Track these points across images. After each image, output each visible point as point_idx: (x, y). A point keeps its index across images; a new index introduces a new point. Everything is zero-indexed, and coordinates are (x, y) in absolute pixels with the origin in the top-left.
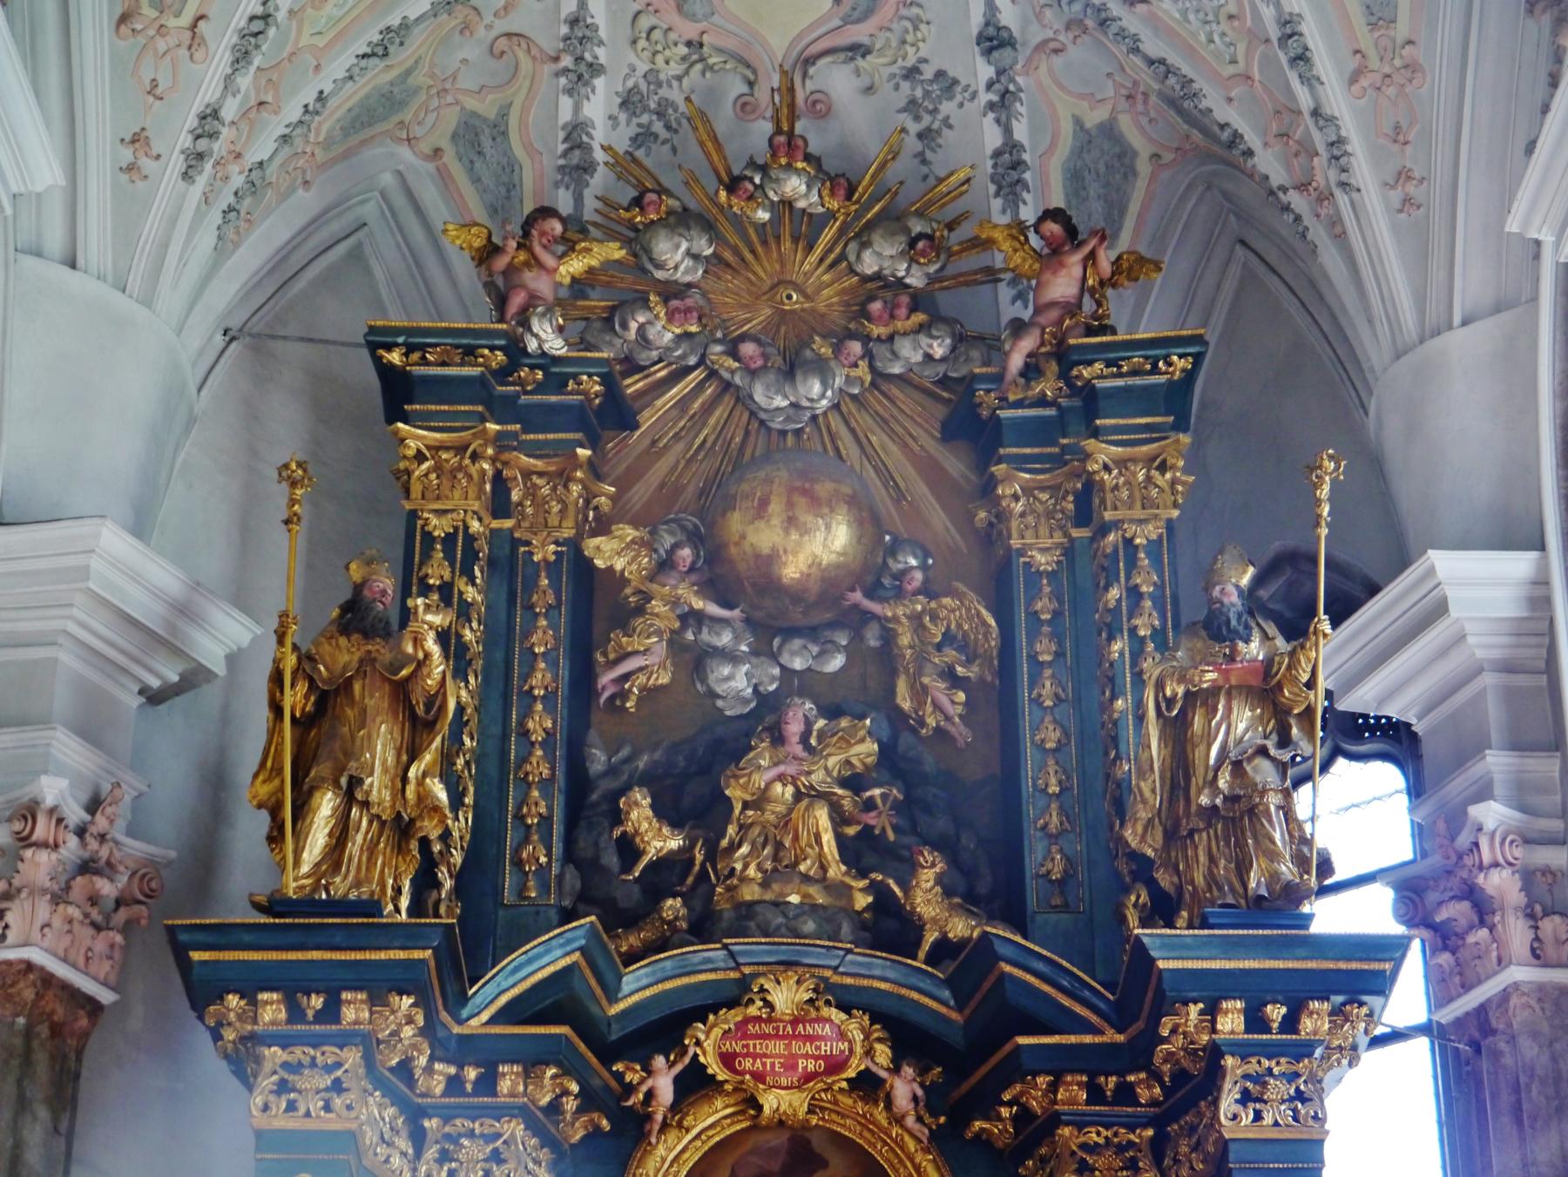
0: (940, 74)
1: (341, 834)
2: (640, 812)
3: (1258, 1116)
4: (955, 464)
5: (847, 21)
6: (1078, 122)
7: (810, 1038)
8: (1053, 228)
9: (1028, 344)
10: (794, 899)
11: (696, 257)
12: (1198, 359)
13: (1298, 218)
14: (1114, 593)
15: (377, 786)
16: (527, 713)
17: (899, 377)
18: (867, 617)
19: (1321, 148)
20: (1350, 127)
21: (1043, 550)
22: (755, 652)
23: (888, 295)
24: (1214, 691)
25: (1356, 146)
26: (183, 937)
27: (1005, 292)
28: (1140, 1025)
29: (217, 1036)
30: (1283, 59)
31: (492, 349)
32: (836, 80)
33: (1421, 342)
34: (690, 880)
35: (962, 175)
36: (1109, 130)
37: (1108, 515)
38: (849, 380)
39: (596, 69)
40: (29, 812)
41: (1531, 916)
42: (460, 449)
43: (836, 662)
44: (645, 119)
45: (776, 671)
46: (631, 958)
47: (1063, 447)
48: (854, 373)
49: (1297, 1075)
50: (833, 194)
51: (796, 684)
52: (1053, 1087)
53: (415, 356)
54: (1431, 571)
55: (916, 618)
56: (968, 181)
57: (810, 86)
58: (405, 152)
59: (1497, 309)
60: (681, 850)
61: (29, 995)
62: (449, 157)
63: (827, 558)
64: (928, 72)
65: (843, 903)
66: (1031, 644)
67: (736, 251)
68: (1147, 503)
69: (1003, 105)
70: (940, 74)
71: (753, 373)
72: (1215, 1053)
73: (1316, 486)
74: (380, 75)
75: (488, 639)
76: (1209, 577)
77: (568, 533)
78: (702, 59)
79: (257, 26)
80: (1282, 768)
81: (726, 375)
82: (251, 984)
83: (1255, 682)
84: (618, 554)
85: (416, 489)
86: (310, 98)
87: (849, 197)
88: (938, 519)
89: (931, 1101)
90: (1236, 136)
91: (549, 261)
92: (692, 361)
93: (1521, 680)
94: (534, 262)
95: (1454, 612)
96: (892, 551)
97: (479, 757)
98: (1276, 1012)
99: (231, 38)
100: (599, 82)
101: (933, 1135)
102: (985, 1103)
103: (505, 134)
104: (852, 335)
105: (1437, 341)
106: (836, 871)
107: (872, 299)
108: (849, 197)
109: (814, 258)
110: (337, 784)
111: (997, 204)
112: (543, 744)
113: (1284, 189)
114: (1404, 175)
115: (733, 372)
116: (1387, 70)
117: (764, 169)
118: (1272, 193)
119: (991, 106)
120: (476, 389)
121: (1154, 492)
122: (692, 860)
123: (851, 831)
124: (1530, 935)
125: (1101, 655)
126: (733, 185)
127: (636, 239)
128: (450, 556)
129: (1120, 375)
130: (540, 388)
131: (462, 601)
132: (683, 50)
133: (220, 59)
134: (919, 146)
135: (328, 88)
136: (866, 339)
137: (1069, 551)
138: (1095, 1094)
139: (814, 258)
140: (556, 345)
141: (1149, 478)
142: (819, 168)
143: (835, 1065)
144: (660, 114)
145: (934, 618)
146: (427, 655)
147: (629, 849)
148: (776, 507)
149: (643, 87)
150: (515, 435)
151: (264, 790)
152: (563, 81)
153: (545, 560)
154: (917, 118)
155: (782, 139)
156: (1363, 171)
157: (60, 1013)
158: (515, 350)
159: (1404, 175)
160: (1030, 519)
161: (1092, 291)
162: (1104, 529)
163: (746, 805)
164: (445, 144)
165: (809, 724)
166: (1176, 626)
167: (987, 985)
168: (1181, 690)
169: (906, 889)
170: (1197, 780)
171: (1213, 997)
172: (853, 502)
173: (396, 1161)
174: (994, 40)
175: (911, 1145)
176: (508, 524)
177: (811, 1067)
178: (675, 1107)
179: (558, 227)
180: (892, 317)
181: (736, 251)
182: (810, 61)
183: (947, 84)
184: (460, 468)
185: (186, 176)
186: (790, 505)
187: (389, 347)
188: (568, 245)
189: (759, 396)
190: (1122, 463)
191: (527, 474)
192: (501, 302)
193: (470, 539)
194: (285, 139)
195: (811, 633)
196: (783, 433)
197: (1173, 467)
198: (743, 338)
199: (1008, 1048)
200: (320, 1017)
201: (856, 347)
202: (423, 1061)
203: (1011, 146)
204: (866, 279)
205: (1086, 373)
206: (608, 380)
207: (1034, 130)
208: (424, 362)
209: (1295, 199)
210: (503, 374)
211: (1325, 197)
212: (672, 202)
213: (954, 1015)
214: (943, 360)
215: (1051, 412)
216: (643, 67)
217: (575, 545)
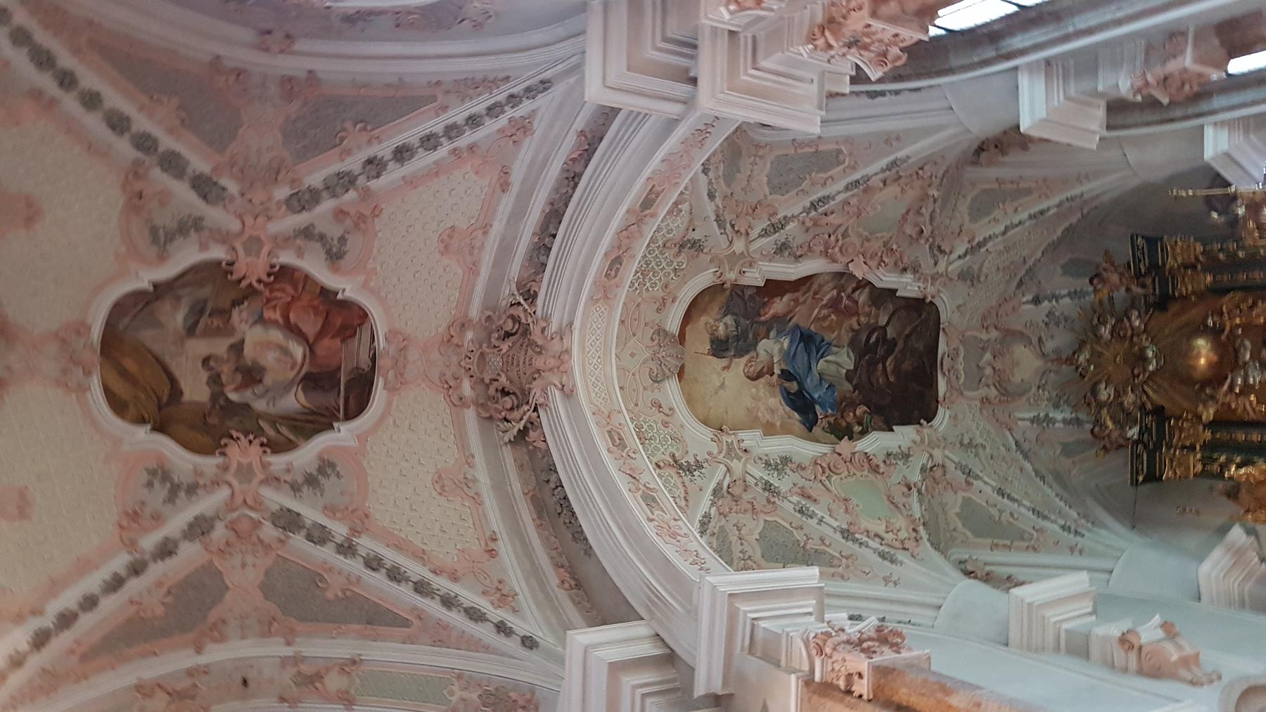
0: (1047, 316)
4: (1174, 307)
5: (1031, 343)
8: (1095, 281)
20: (1063, 197)
32: (1050, 346)
39: (1047, 415)
42: (1171, 461)
43: (1248, 343)
57: (1051, 354)
59: (1122, 148)
71: (1145, 370)
77: (1201, 428)
86: (1057, 500)
88: (1194, 314)
91: (1107, 431)
94: (1109, 435)
96: (1206, 326)
99: (1040, 520)
100: (1051, 415)
105: (1131, 164)
117: (1077, 368)
130: (1150, 434)
133: (1046, 524)
135: (1054, 494)
137: (1205, 270)
152: (1051, 426)
156: (1076, 191)
158: (1137, 442)
174: (1036, 301)
176: (1198, 447)
185: (1083, 536)
187: (1137, 481)
188: (1103, 426)
189: (1151, 368)
192: (1120, 446)
194: (1070, 507)
195: (1236, 352)
198: (1133, 372)
201: (1135, 339)
204: (1112, 335)
205: (1143, 270)
206: (1147, 414)
210: (1146, 447)
211: (1085, 202)
215: (1157, 279)
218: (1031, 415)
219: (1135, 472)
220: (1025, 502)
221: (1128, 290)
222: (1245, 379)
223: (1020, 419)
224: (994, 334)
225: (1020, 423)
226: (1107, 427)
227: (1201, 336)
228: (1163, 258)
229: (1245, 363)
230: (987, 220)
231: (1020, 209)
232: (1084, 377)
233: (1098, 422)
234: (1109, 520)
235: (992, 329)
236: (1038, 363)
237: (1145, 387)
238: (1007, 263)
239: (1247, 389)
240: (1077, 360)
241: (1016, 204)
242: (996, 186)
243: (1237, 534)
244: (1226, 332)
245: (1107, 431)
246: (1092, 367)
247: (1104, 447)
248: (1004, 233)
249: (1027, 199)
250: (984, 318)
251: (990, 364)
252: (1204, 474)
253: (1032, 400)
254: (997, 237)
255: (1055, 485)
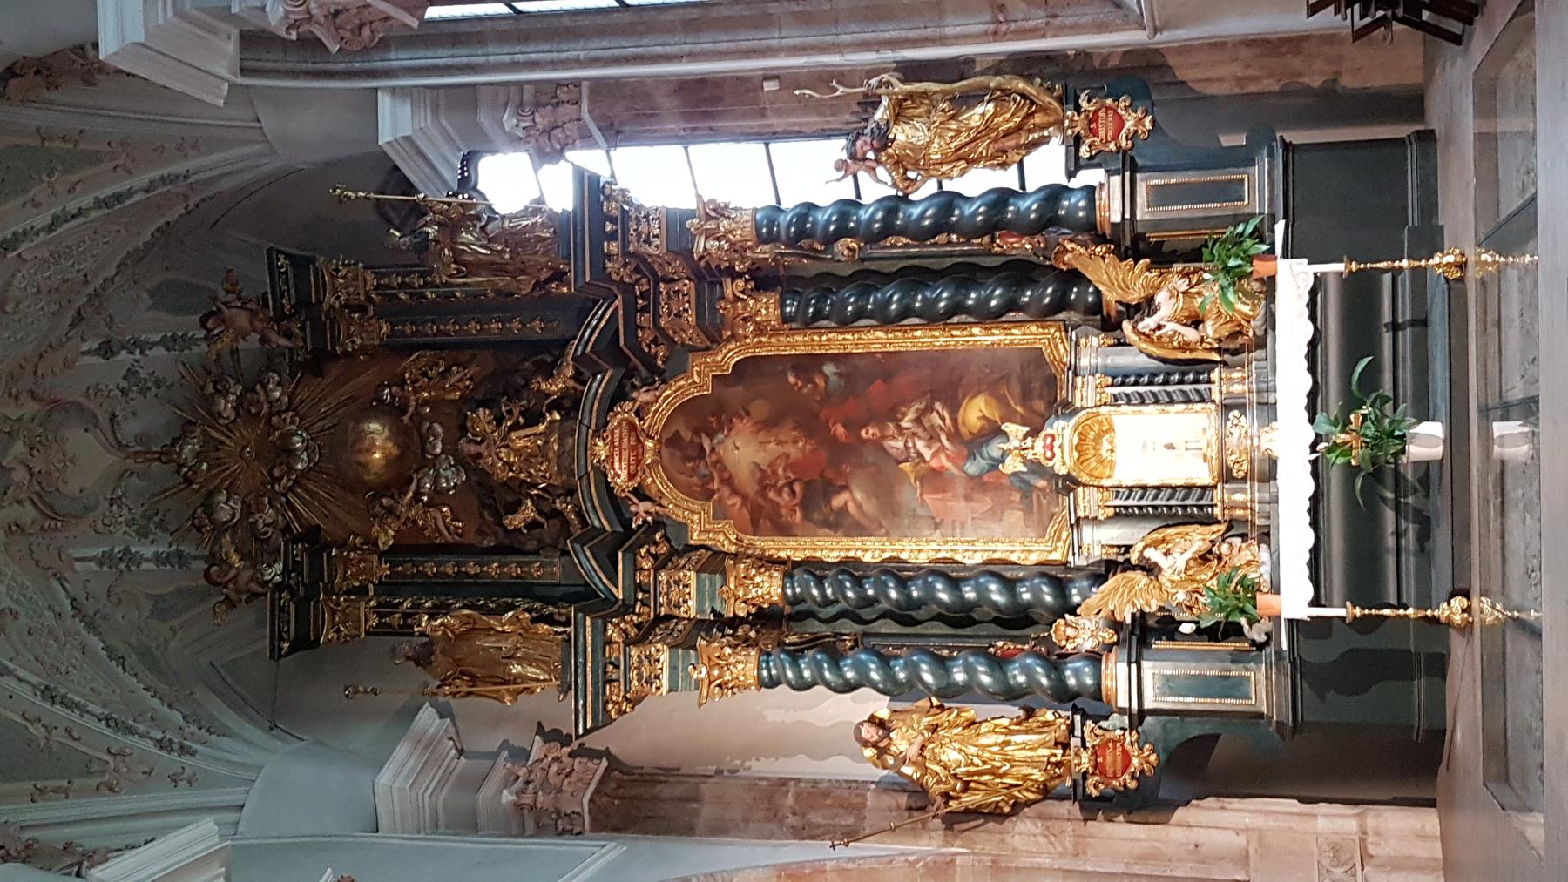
0: (125, 378)
1: (526, 660)
2: (516, 521)
3: (656, 236)
4: (334, 371)
5: (96, 425)
6: (150, 308)
7: (621, 439)
8: (210, 324)
9: (274, 337)
10: (556, 447)
11: (228, 500)
12: (279, 252)
13: (203, 200)
14: (402, 296)
15: (506, 645)
16: (466, 573)
17: (289, 398)
18: (416, 413)
19: (166, 189)
20: (156, 174)
21: (380, 328)
22: (434, 466)
23: (246, 404)
24: (452, 249)
25: (165, 171)
26: (581, 731)
27: (241, 345)
28: (614, 289)
29: (625, 712)
30: (119, 206)
31: (280, 598)
32: (130, 429)
33: (268, 142)
34: (546, 496)
35: (181, 367)
36: (152, 294)
37: (362, 298)
38: (292, 422)
39: (126, 551)
40: (519, 806)
41: (557, 104)
42: (333, 612)
43: (438, 429)
44: (152, 526)
45: (443, 457)
46: (583, 522)
47: (327, 318)
48: (288, 421)
49: (637, 218)
50: (191, 432)
51: (451, 448)
52: (642, 328)
53: (285, 635)
54: (389, 143)
55: (415, 391)
56: (184, 365)
58: (173, 644)
60: (532, 500)
61: (605, 799)
62: (176, 623)
63: (387, 433)
64: (124, 384)
65: (557, 425)
66: (427, 335)
67: (224, 480)
68: (355, 278)
69: (143, 346)
70: (125, 378)
71: (291, 469)
72: (626, 254)
73: (349, 198)
74: (132, 660)
75: (430, 596)
76: (396, 250)
77: (375, 557)
78: (120, 498)
79: (112, 723)
80: (490, 219)
81: (291, 483)
82: (601, 702)
83: (448, 231)
84: (386, 533)
85: (354, 632)
86: (148, 694)
87: (194, 424)
88: (366, 378)
89: (648, 383)
90: (158, 230)
91: (233, 572)
92: (283, 499)
93: (442, 103)
95: (408, 133)
96: (381, 401)
97: (489, 597)
98: (609, 227)
100: (133, 550)
101: (664, 382)
102: (649, 361)
103: (161, 596)
104: (269, 421)
106: (542, 427)
107: (249, 411)
108: (194, 424)
109: (228, 442)
110: (507, 664)
111: (195, 349)
112: (482, 567)
113: (186, 208)
114: (180, 148)
115: (289, 480)
116: (124, 155)
117: (180, 466)
118: (189, 213)
119: (142, 353)
120: (302, 606)
121: (350, 275)
122: (537, 495)
123: (521, 420)
124: (566, 105)
125: (433, 301)
126: (189, 481)
127: (220, 529)
128: (389, 615)
129: (288, 290)
130: (300, 574)
131: (411, 608)
132: (115, 507)
133: (132, 740)
134: (163, 388)
136: (270, 415)
137: (379, 316)
138: (644, 310)
139: (228, 442)
140: (278, 567)
141: (342, 278)
142: (179, 438)
143: (632, 427)
144: (150, 518)
145: (413, 382)
146: (442, 624)
147: (532, 525)
148: (361, 458)
149: (135, 527)
150: (325, 585)
151: (508, 698)
153: (389, 569)
154: (149, 389)
155: (163, 458)
156: (179, 168)
157: (613, 785)
158: (280, 587)
159: (180, 148)
160: (364, 335)
161: (244, 303)
162: (369, 299)
163: (511, 470)
164: (167, 625)
165: (470, 441)
166: (417, 266)
167: (594, 357)
168: (453, 266)
169: (548, 396)
170: (497, 259)
171: (600, 257)
172: (358, 421)
173: (680, 627)
174: (107, 350)
175: (667, 392)
177: (632, 439)
178: (653, 501)
179: (214, 568)
180: (258, 402)
181: (224, 480)
182: (119, 443)
183: (130, 374)
184: (343, 611)
185: (193, 753)
186: (359, 451)
187: (281, 649)
188: (225, 563)
190: (335, 291)
191: (345, 579)
193: (379, 605)
194: (170, 706)
195: (423, 439)
196: (320, 455)
197: (337, 265)
198: (271, 475)
199: (625, 349)
200: (617, 667)
201: (275, 419)
202: (635, 618)
203: (162, 342)
204: (238, 415)
206: (295, 542)
207: (155, 331)
208: (288, 631)
209: (191, 204)
210: (293, 592)
212: (199, 511)
213: (609, 374)
214: (280, 375)
216: (125, 528)
217: (381, 554)
218: (97, 551)
219: (277, 637)
220: (91, 707)
221: (264, 340)
222: (436, 482)
223: (78, 560)
224: (30, 408)
225: (78, 566)
226: (231, 566)
227: (376, 419)
228: (317, 293)
229: (437, 457)
230: (21, 200)
231: (78, 188)
232: (191, 483)
233: (213, 558)
234: (231, 719)
235: (24, 398)
236: (110, 459)
237: (291, 497)
238: (55, 282)
239: (438, 493)
240: (179, 454)
241: (73, 178)
242: (36, 142)
243: (427, 717)
244: (411, 409)
245: (233, 572)
246: (205, 466)
247: (227, 597)
248: (51, 228)
249: (88, 172)
250: (12, 378)
251: (22, 462)
252: (383, 630)
253: (100, 524)
254: (37, 234)
255: (140, 668)
